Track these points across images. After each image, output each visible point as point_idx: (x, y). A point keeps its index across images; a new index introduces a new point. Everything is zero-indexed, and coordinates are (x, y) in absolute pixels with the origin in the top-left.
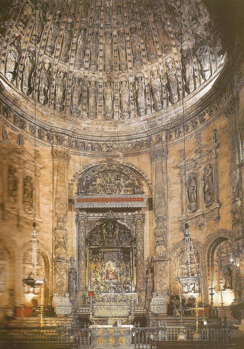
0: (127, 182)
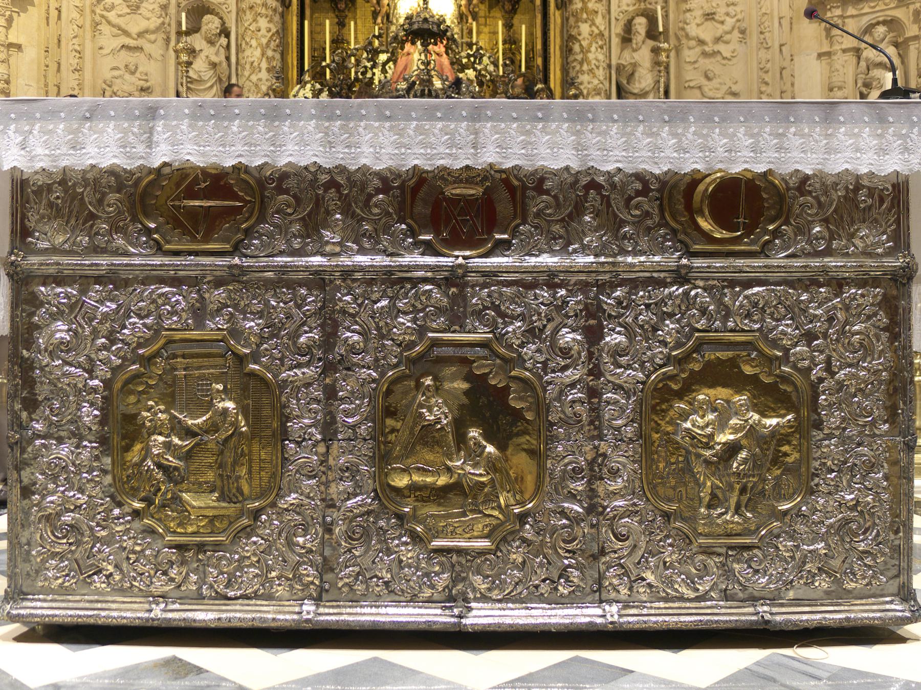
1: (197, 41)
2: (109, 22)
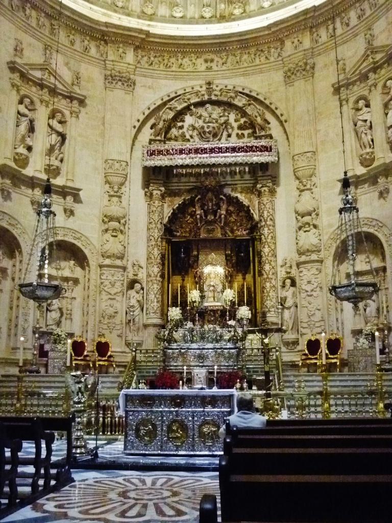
0: (242, 120)
1: (132, 293)
2: (105, 291)
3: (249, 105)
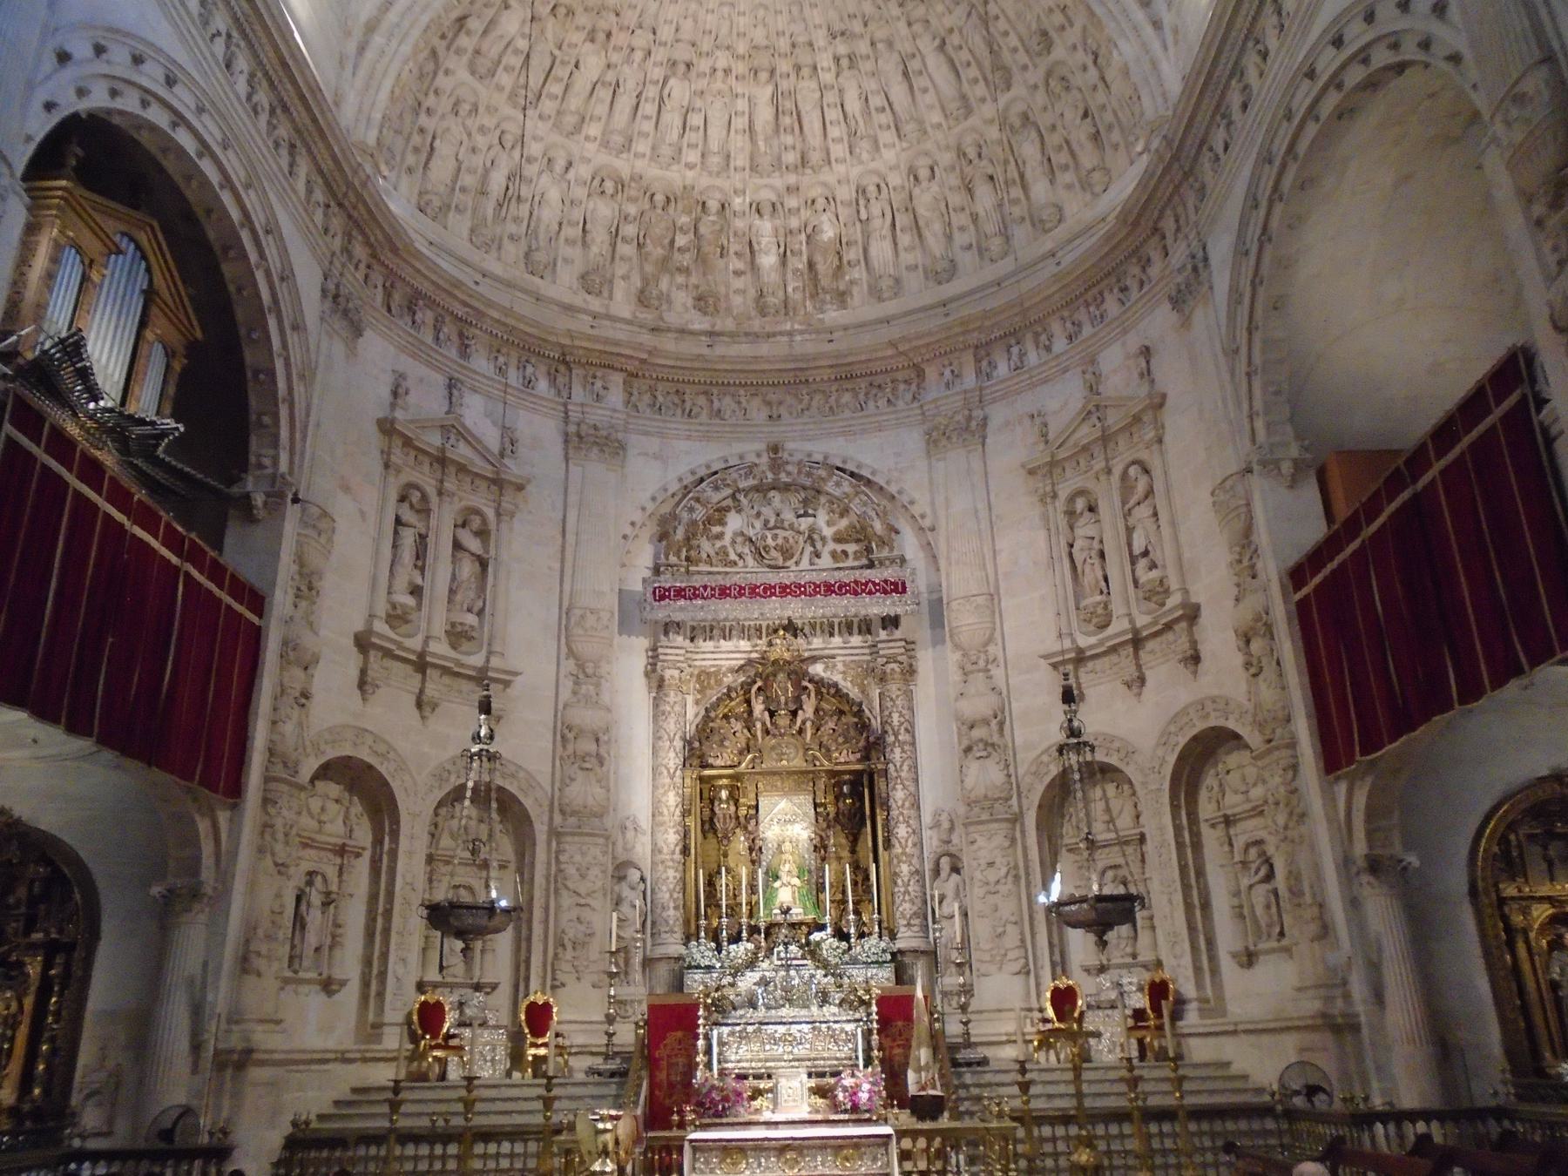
0: (844, 523)
3: (857, 493)
